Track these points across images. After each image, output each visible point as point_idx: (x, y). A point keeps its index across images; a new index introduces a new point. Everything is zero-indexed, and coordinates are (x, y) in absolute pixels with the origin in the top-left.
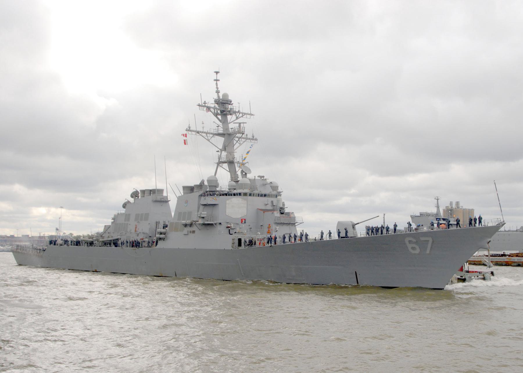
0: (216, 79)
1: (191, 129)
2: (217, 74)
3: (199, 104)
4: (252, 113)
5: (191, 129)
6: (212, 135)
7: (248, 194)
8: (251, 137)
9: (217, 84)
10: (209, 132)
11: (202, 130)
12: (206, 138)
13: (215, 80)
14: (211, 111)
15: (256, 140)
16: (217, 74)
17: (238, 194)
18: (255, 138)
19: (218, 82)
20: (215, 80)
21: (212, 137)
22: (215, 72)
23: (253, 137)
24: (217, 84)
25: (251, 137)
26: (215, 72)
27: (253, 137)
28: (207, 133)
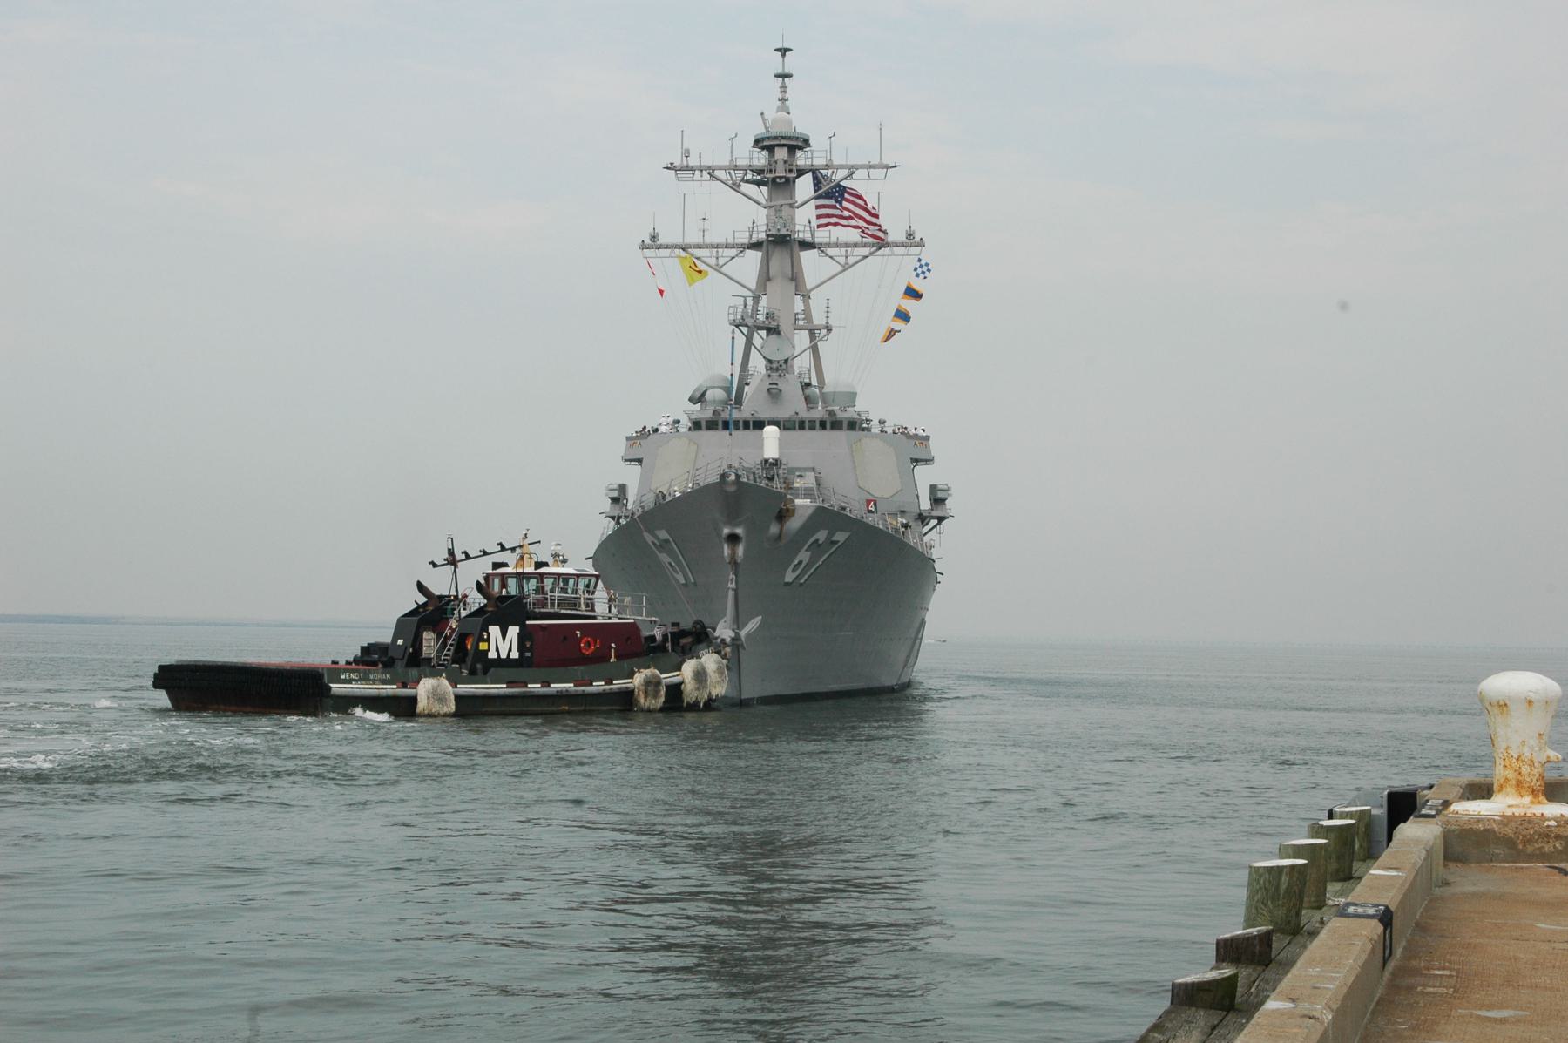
0: (780, 71)
1: (662, 240)
2: (784, 55)
3: (672, 164)
4: (885, 162)
5: (662, 240)
6: (733, 252)
7: (704, 425)
8: (902, 238)
9: (784, 88)
10: (730, 241)
11: (700, 241)
12: (713, 262)
13: (778, 76)
15: (921, 244)
16: (784, 55)
17: (741, 424)
18: (917, 239)
19: (786, 79)
20: (778, 76)
21: (733, 258)
22: (777, 50)
23: (910, 235)
24: (784, 88)
25: (902, 238)
26: (777, 50)
27: (910, 235)
28: (717, 247)
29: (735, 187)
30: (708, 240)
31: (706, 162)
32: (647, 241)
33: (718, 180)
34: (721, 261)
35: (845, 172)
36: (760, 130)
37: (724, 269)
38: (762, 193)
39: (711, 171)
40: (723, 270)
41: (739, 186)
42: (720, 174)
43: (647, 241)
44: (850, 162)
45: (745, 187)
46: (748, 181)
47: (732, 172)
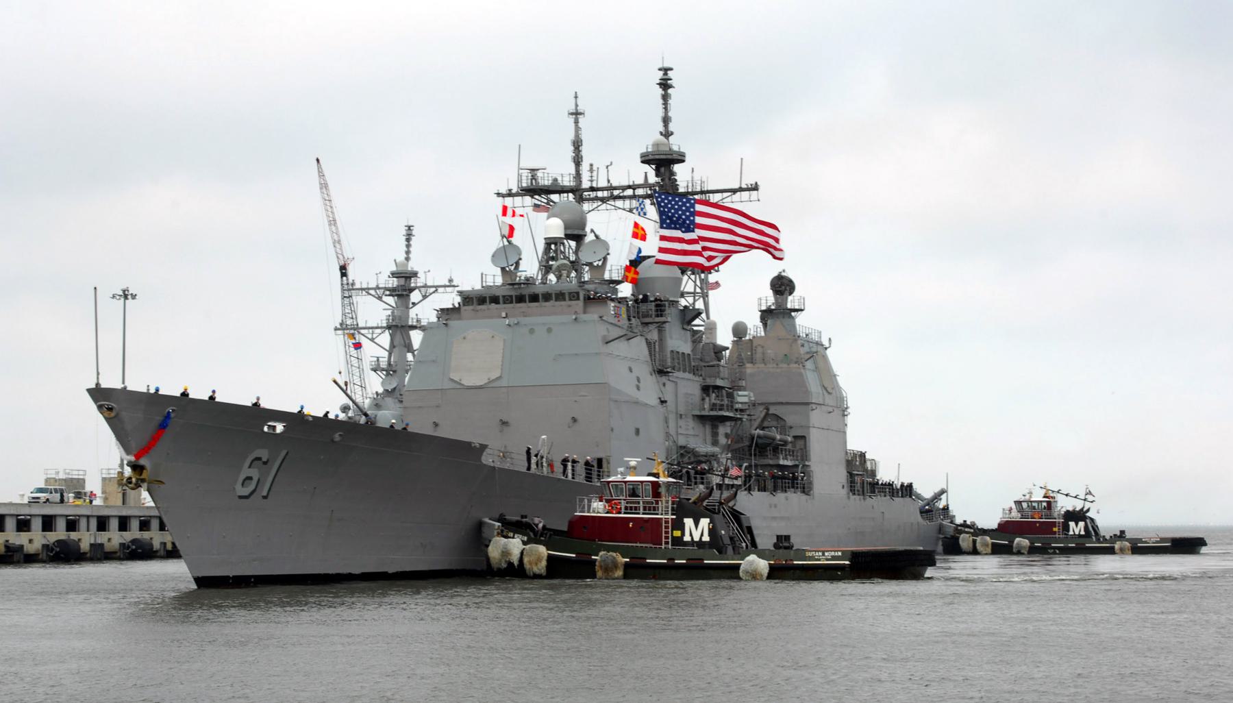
10: (380, 325)
12: (370, 336)
14: (371, 294)
28: (372, 328)
29: (380, 298)
30: (368, 325)
31: (364, 286)
32: (339, 326)
33: (371, 294)
34: (375, 336)
35: (434, 289)
36: (394, 269)
37: (375, 340)
38: (391, 300)
39: (367, 290)
40: (375, 340)
41: (381, 298)
42: (372, 292)
43: (339, 326)
44: (436, 284)
45: (385, 298)
46: (386, 295)
47: (378, 291)
